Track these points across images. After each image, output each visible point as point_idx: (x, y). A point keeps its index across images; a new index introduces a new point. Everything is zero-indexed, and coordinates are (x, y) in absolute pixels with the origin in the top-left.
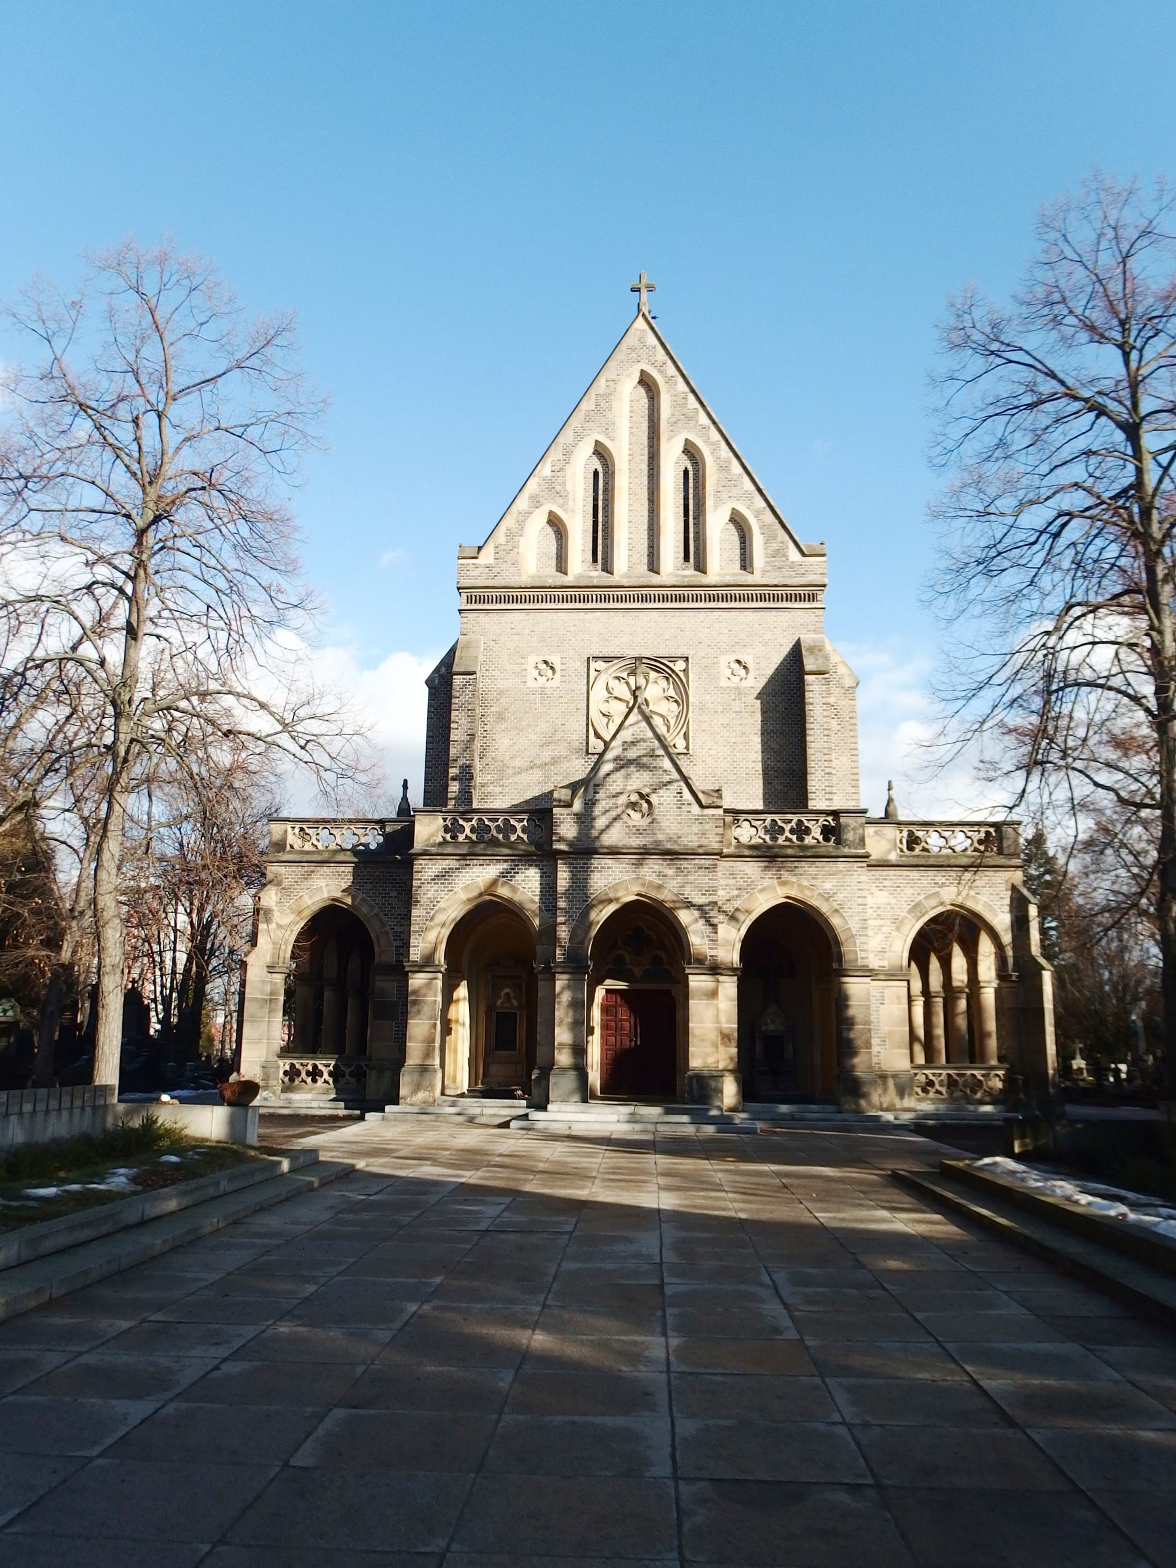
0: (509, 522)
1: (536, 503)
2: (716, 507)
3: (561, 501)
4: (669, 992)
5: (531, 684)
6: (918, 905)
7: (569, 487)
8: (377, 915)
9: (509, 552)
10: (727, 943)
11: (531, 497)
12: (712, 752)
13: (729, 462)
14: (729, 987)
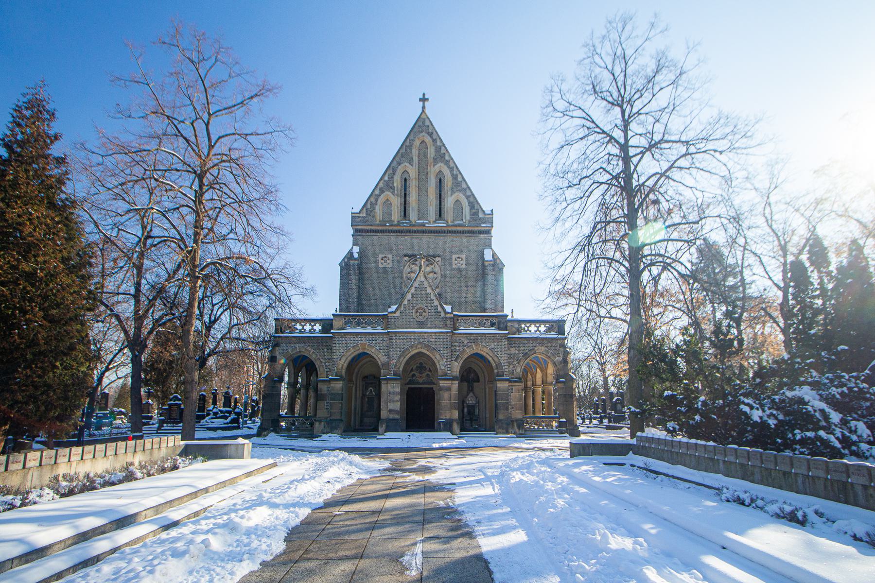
0: (372, 199)
10: (456, 367)
11: (380, 189)
13: (457, 175)
14: (455, 385)
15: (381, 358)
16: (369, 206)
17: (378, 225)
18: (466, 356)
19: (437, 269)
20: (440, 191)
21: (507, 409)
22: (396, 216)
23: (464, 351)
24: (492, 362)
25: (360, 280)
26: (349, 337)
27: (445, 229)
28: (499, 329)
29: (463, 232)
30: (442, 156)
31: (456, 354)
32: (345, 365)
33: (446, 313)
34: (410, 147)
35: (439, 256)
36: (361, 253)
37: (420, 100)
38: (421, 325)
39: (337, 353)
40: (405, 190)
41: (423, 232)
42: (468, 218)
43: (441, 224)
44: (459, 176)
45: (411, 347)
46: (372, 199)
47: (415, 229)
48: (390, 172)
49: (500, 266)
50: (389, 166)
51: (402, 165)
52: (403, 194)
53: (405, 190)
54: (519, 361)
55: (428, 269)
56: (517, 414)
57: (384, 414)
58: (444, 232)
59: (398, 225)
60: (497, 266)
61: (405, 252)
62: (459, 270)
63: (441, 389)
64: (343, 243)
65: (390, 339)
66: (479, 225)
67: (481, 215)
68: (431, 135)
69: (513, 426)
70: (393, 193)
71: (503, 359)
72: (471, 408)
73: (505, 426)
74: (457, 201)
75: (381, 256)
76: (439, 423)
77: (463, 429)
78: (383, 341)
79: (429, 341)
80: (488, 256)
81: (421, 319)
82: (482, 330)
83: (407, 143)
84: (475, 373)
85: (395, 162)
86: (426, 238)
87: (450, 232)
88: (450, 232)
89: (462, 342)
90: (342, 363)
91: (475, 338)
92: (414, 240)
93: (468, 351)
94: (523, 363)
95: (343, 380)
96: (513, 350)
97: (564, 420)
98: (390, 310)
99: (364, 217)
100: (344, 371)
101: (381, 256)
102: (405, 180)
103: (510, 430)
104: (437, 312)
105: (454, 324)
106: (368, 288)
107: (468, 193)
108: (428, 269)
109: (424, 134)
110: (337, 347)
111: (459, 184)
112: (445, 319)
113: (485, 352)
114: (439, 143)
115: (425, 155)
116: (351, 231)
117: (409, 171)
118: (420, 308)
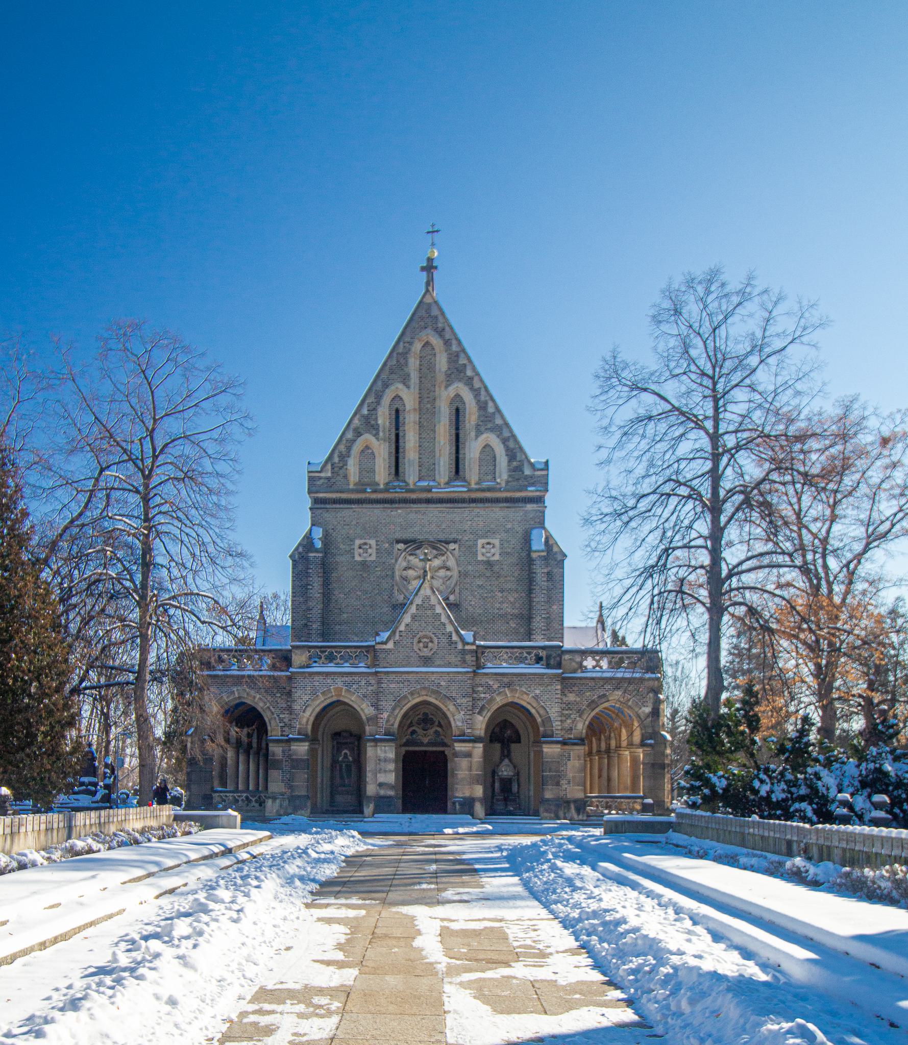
1: (358, 433)
2: (477, 437)
3: (374, 432)
4: (443, 752)
5: (357, 558)
6: (593, 701)
7: (380, 422)
8: (268, 708)
9: (341, 468)
10: (480, 724)
12: (473, 603)
14: (478, 750)
15: (366, 710)
16: (336, 459)
17: (352, 491)
18: (495, 707)
19: (451, 563)
20: (457, 429)
21: (558, 784)
22: (382, 474)
23: (492, 700)
24: (537, 716)
25: (326, 583)
26: (317, 678)
27: (466, 496)
28: (548, 666)
29: (497, 501)
30: (461, 370)
31: (480, 704)
32: (312, 719)
33: (465, 643)
34: (405, 354)
35: (455, 542)
36: (326, 539)
37: (423, 269)
38: (427, 661)
39: (299, 701)
40: (397, 429)
41: (428, 501)
42: (505, 476)
43: (458, 489)
44: (490, 404)
45: (412, 694)
46: (342, 448)
47: (414, 496)
48: (371, 399)
49: (559, 558)
50: (370, 389)
51: (393, 388)
52: (393, 437)
53: (397, 429)
54: (581, 713)
55: (437, 563)
56: (575, 792)
57: (371, 789)
58: (463, 501)
59: (386, 490)
60: (554, 558)
61: (398, 536)
62: (489, 564)
63: (456, 755)
64: (297, 522)
65: (379, 682)
66: (526, 486)
67: (527, 471)
68: (440, 332)
69: (569, 809)
70: (376, 435)
71: (554, 712)
72: (506, 784)
73: (553, 808)
74: (487, 446)
75: (358, 542)
76: (454, 803)
77: (491, 812)
78: (368, 684)
79: (439, 685)
80: (538, 544)
81: (426, 652)
82: (522, 669)
83: (400, 349)
84: (507, 732)
85: (380, 383)
86: (433, 511)
87: (473, 501)
88: (473, 501)
89: (489, 687)
90: (307, 717)
91: (509, 681)
92: (412, 516)
93: (498, 699)
94: (588, 716)
95: (309, 741)
96: (571, 697)
97: (650, 801)
98: (378, 639)
99: (328, 479)
100: (310, 727)
101: (358, 542)
102: (397, 411)
103: (561, 814)
104: (451, 643)
105: (478, 659)
106: (338, 595)
107: (506, 434)
108: (437, 563)
109: (429, 331)
110: (299, 693)
111: (492, 419)
112: (463, 652)
113: (525, 700)
114: (455, 348)
115: (431, 368)
116: (309, 503)
117: (404, 397)
118: (425, 637)
